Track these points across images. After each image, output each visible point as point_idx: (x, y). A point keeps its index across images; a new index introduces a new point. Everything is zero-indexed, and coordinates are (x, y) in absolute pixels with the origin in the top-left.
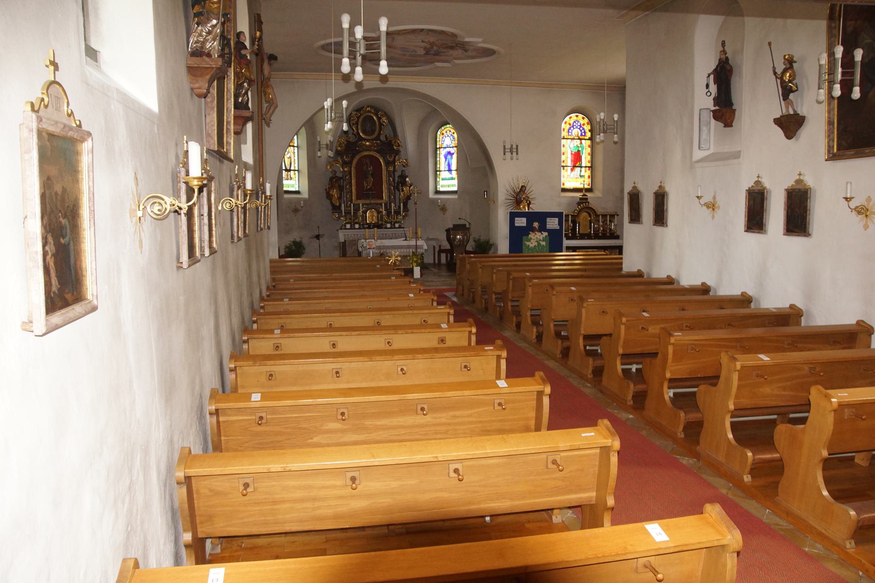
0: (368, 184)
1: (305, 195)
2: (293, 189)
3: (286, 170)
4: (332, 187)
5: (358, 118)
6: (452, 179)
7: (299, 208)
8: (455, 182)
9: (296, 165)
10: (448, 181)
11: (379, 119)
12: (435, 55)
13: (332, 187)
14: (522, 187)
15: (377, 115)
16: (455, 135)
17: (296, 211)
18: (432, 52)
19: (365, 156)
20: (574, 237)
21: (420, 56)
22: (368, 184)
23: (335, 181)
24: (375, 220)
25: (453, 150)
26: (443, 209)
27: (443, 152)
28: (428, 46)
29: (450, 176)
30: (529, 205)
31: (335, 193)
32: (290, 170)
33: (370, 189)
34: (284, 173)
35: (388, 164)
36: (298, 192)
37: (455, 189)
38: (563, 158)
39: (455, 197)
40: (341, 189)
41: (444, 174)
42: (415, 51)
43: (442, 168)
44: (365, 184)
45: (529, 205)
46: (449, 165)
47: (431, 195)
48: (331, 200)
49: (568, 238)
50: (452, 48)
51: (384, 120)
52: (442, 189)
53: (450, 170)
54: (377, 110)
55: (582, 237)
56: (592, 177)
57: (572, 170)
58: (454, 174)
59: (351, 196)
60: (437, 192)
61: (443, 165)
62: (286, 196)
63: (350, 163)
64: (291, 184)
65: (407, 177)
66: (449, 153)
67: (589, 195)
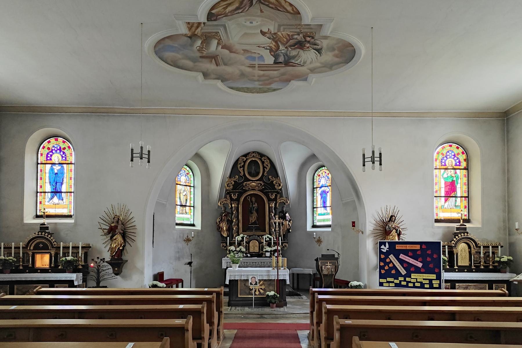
0: (253, 218)
1: (198, 227)
2: (189, 223)
3: (181, 206)
4: (221, 220)
5: (245, 162)
6: (328, 214)
7: (191, 238)
8: (330, 217)
9: (192, 202)
10: (322, 216)
11: (263, 163)
12: (287, 63)
13: (221, 220)
14: (392, 216)
15: (261, 159)
16: (330, 176)
17: (188, 240)
18: (281, 59)
19: (251, 195)
20: (451, 269)
21: (268, 66)
22: (253, 218)
23: (226, 215)
24: (257, 250)
25: (327, 189)
26: (319, 241)
27: (319, 191)
28: (273, 45)
29: (325, 211)
30: (399, 235)
31: (224, 226)
32: (185, 206)
33: (255, 223)
34: (178, 208)
35: (270, 200)
36: (193, 225)
37: (330, 223)
38: (436, 188)
39: (329, 229)
40: (230, 222)
41: (321, 210)
42: (261, 58)
43: (319, 205)
44: (251, 219)
45: (399, 235)
46: (324, 202)
47: (309, 228)
48: (220, 232)
49: (447, 271)
50: (300, 45)
51: (267, 163)
52: (318, 224)
53: (325, 207)
54: (261, 155)
55: (462, 269)
56: (468, 207)
57: (446, 200)
58: (329, 209)
59: (238, 229)
60: (314, 226)
61: (319, 202)
62: (177, 227)
63: (238, 200)
64: (182, 216)
65: (286, 213)
66: (324, 192)
67: (468, 225)
